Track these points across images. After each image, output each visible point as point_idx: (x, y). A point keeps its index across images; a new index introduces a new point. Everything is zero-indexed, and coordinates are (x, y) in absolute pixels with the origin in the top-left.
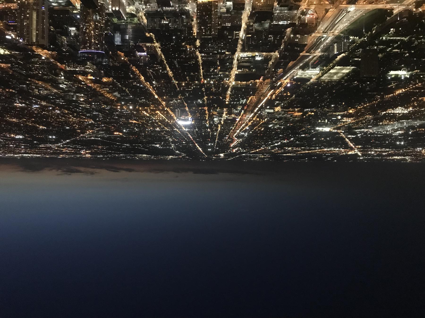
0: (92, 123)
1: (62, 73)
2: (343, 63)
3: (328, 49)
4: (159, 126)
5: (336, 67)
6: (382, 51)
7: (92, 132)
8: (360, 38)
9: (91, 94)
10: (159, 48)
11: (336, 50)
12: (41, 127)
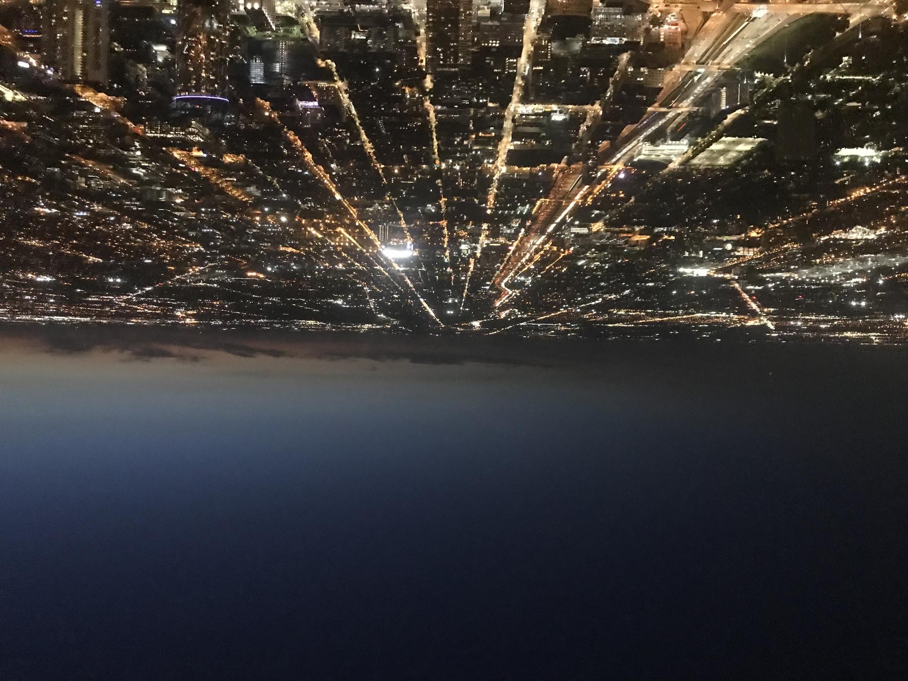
0: (200, 251)
1: (137, 144)
2: (740, 129)
3: (708, 98)
4: (344, 260)
5: (724, 139)
6: (822, 105)
7: (200, 271)
8: (776, 76)
9: (198, 189)
10: (346, 91)
11: (724, 102)
12: (91, 259)
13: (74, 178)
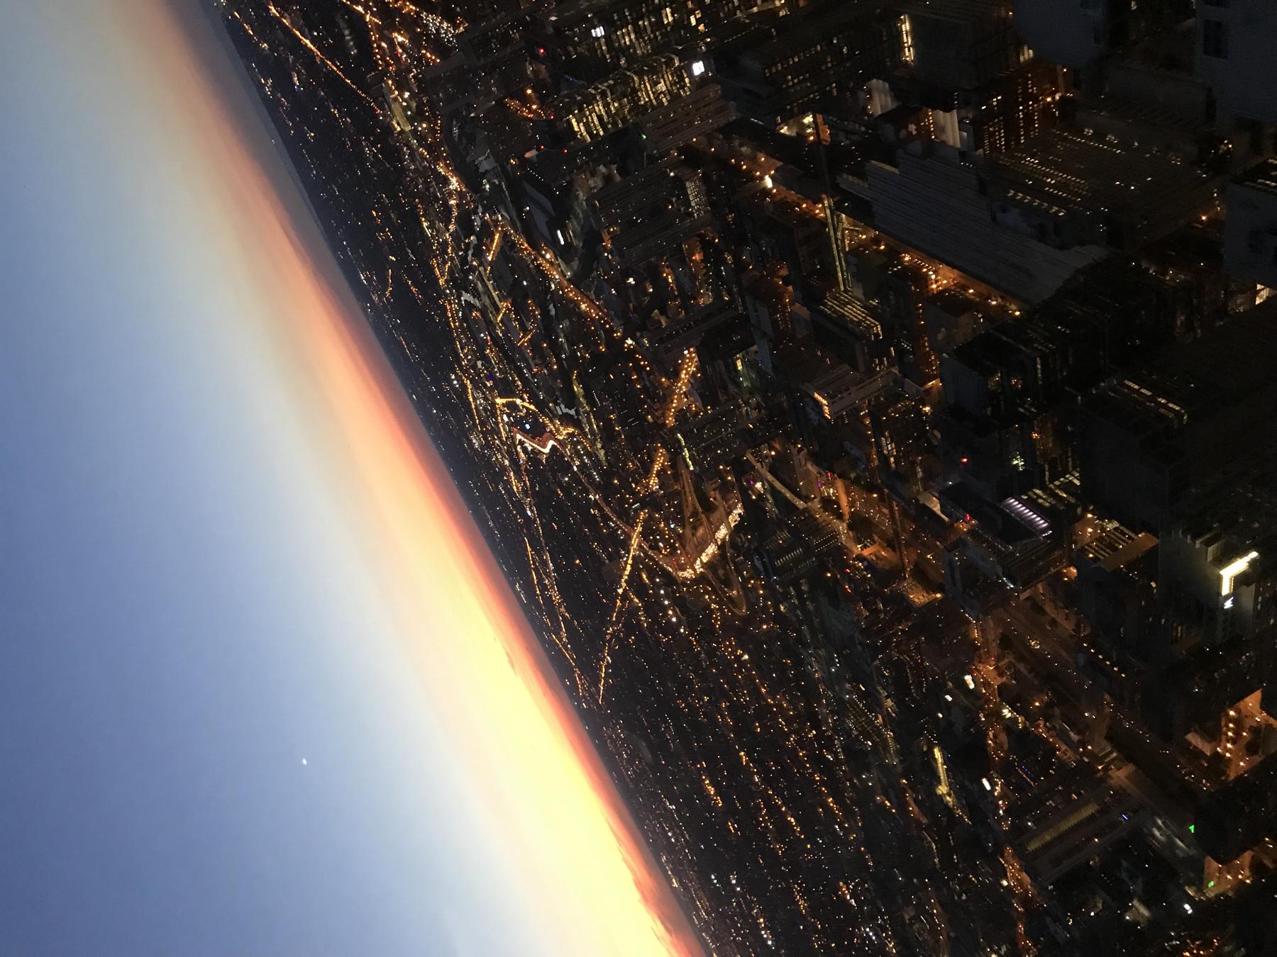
13: (908, 902)
